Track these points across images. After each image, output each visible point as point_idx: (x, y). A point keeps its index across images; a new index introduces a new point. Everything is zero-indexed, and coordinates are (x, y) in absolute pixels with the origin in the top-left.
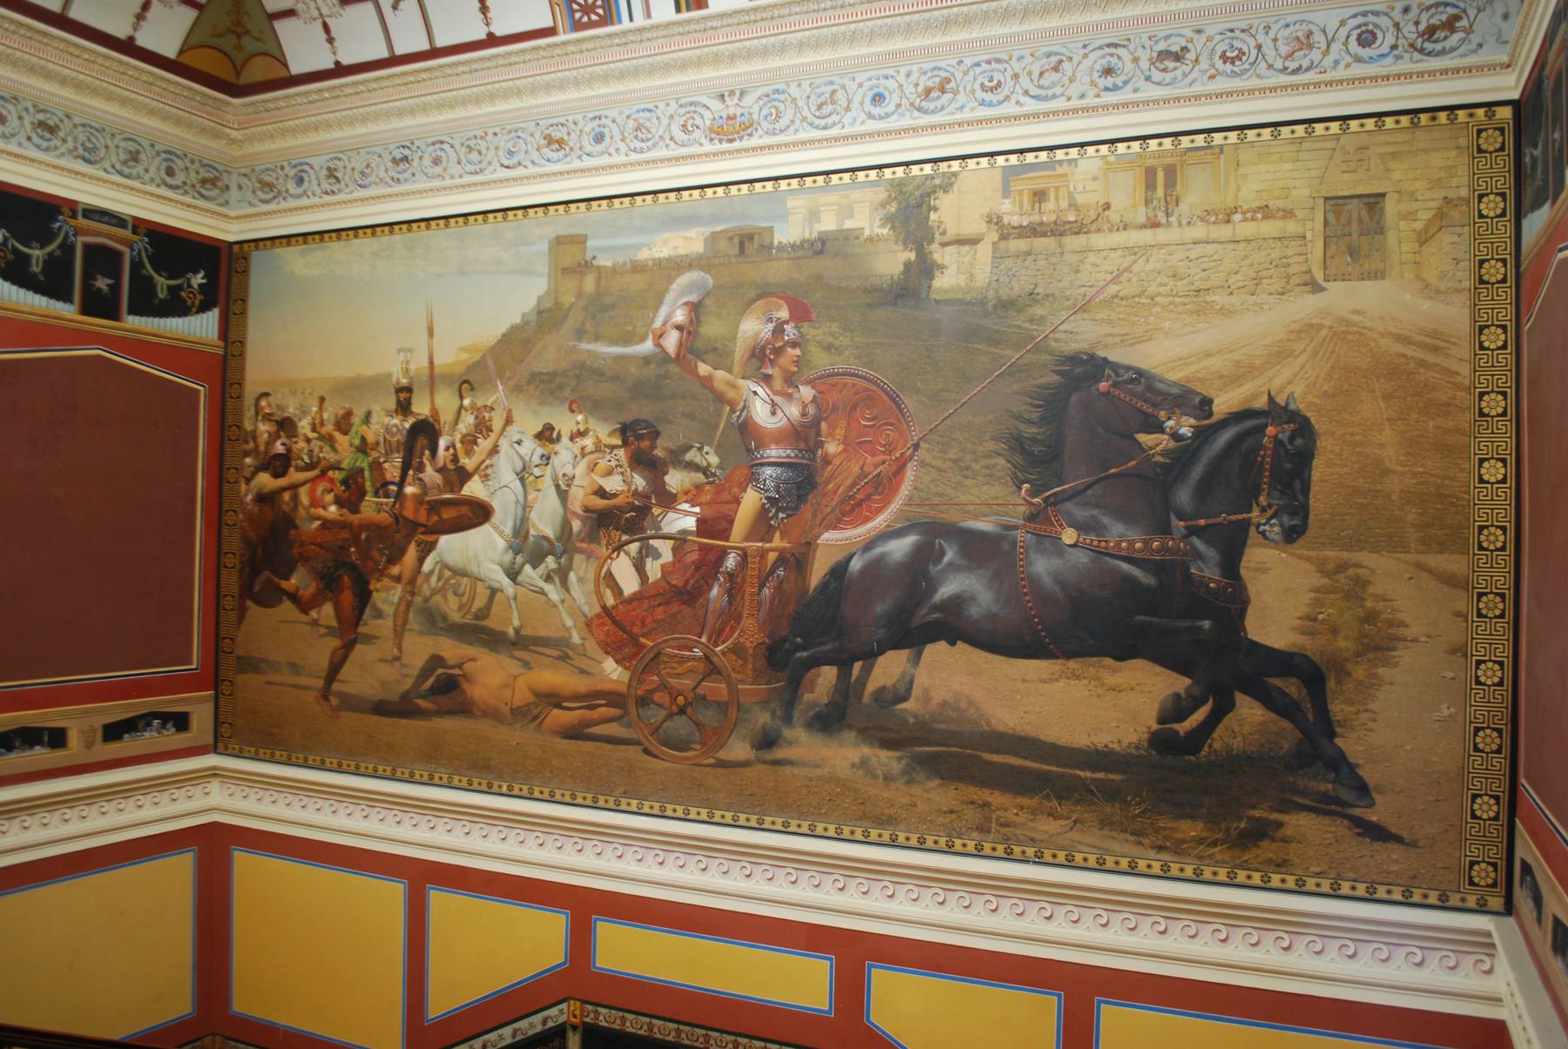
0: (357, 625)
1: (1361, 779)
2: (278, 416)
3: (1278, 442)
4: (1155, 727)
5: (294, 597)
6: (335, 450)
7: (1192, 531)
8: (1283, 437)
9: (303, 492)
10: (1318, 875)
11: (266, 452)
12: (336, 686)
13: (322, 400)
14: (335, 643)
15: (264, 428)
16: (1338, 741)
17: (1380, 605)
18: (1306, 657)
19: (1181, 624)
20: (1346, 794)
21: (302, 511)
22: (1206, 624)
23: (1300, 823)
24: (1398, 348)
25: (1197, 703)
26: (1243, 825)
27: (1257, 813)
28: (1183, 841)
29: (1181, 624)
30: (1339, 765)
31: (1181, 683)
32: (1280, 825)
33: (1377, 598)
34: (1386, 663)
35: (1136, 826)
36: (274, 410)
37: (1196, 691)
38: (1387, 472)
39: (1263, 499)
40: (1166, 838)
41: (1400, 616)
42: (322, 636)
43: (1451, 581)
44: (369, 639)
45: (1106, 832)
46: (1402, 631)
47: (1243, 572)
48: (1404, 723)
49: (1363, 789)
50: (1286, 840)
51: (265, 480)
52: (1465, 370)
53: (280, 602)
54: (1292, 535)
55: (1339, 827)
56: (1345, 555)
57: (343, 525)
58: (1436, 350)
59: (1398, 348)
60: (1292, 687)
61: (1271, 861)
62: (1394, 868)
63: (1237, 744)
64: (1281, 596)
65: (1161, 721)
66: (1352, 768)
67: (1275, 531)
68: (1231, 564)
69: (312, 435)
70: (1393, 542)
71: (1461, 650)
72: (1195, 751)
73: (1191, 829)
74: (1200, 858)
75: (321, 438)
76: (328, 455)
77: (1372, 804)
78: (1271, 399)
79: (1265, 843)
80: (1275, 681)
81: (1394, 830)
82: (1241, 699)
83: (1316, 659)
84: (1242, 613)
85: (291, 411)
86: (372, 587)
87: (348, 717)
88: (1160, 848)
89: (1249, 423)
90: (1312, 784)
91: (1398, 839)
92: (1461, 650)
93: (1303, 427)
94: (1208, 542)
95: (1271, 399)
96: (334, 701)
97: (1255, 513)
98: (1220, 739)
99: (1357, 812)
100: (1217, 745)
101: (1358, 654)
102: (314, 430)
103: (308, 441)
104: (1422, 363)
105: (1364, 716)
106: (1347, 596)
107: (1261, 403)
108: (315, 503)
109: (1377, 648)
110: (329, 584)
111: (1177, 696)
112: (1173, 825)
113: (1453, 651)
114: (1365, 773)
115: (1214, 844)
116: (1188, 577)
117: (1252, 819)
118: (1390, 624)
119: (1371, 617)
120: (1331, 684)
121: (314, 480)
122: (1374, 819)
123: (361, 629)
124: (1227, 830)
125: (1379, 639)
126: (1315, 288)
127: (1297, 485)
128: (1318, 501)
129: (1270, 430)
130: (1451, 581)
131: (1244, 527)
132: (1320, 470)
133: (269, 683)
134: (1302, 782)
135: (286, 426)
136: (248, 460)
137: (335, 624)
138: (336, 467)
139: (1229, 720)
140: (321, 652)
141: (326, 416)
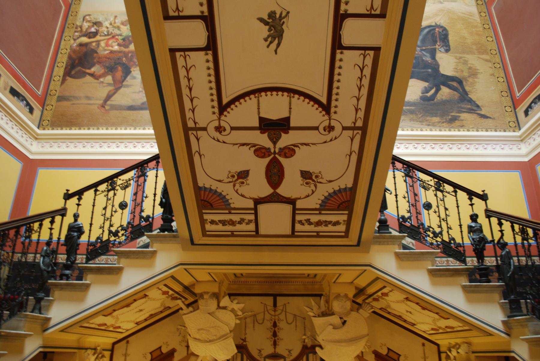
0: (123, 81)
1: (477, 104)
2: (94, 21)
3: (439, 32)
4: (421, 95)
5: (92, 75)
6: (120, 31)
7: (422, 50)
8: (441, 31)
9: (103, 44)
10: (472, 128)
11: (86, 31)
12: (109, 103)
13: (116, 17)
14: (111, 88)
15: (86, 25)
16: (469, 96)
17: (472, 66)
18: (457, 77)
19: (423, 70)
20: (475, 108)
21: (100, 48)
22: (430, 70)
23: (464, 116)
24: (463, 15)
25: (431, 89)
26: (450, 117)
27: (453, 114)
28: (434, 123)
29: (423, 70)
30: (471, 101)
31: (426, 84)
32: (459, 116)
33: (471, 64)
34: (476, 78)
35: (421, 120)
36: (93, 19)
37: (431, 86)
38: (466, 39)
39: (438, 44)
40: (430, 122)
41: (477, 68)
42: (104, 87)
43: (487, 61)
44: (127, 86)
45: (412, 122)
46: (478, 71)
47: (437, 59)
48: (486, 89)
49: (478, 106)
50: (462, 120)
51: (84, 40)
52: (479, 20)
53: (85, 76)
54: (447, 51)
55: (475, 116)
56: (461, 55)
57: (120, 52)
58: (471, 16)
59: (463, 15)
60: (455, 84)
61: (459, 126)
62: (491, 125)
63: (444, 98)
64: (447, 64)
65: (422, 93)
66: (474, 102)
67: (442, 50)
68: (433, 57)
69: (108, 26)
70: (472, 53)
71: (493, 75)
72: (433, 100)
73: (436, 119)
74: (440, 127)
75: (114, 27)
76: (116, 31)
77: (481, 110)
78: (436, 24)
79: (457, 121)
80: (450, 83)
81: (488, 116)
82: (442, 87)
83: (459, 77)
84: (439, 67)
85: (100, 19)
86: (132, 70)
87: (113, 113)
88: (429, 125)
89: (431, 28)
90: (465, 106)
91: (490, 118)
92: (493, 75)
93: (445, 29)
94: (427, 52)
95: (436, 24)
96: (107, 107)
97: (437, 46)
98: (439, 97)
99: (478, 112)
100: (439, 98)
101: (469, 76)
102: (111, 24)
103: (107, 28)
104: (469, 18)
105: (474, 90)
106: (463, 64)
107: (433, 24)
108: (107, 45)
109: (473, 75)
110: (111, 70)
111: (425, 87)
112: (430, 119)
113: (491, 75)
114: (477, 103)
115: (443, 123)
116: (423, 60)
117: (452, 116)
118: (475, 69)
119: (470, 68)
120: (464, 83)
121: (109, 39)
122: (483, 113)
123: (124, 83)
124: (446, 119)
125: (474, 73)
126: (441, 3)
127: (446, 41)
128: (451, 43)
129: (437, 29)
130: (487, 61)
131: (435, 49)
132: (450, 38)
133: (73, 104)
134: (463, 106)
135: (97, 24)
136: (76, 34)
137: (112, 82)
138: (121, 35)
139: (440, 92)
140: (104, 92)
141: (117, 21)
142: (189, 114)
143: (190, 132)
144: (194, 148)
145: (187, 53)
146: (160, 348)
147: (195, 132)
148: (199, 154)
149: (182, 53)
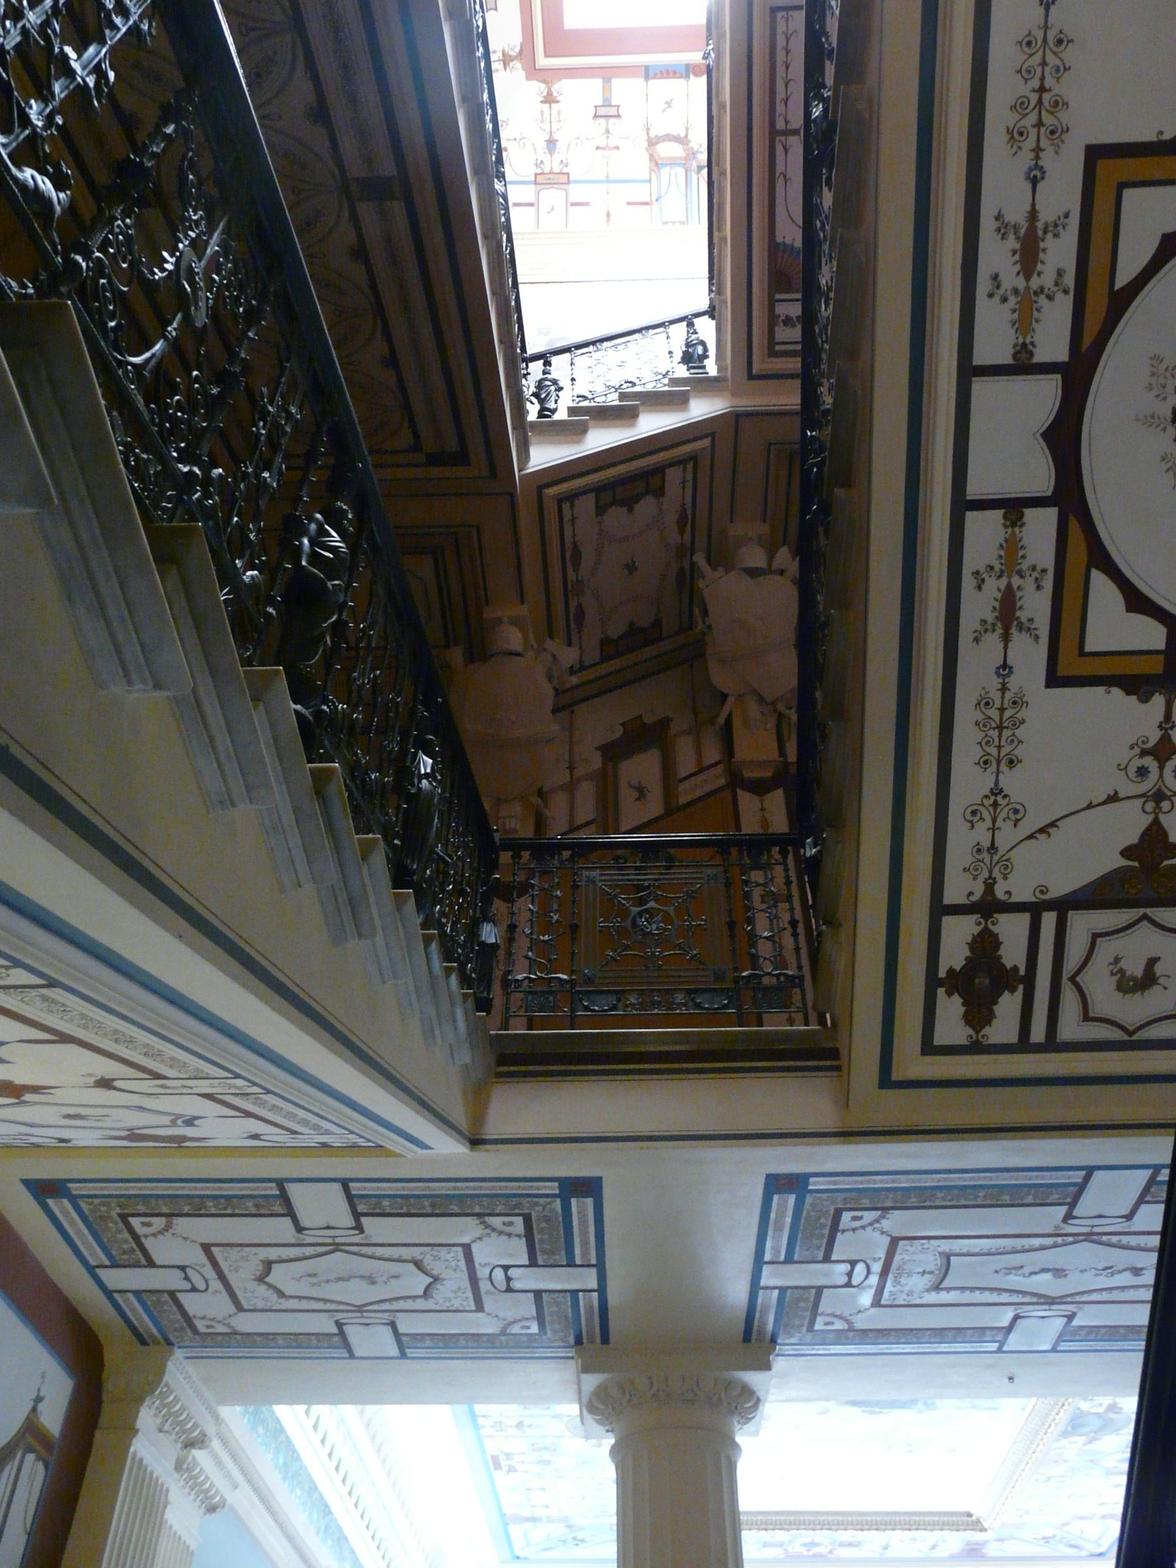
142: (780, 108)
143: (778, 139)
144: (780, 168)
145: (790, 13)
146: (641, 716)
147: (783, 138)
148: (785, 177)
149: (785, 13)
